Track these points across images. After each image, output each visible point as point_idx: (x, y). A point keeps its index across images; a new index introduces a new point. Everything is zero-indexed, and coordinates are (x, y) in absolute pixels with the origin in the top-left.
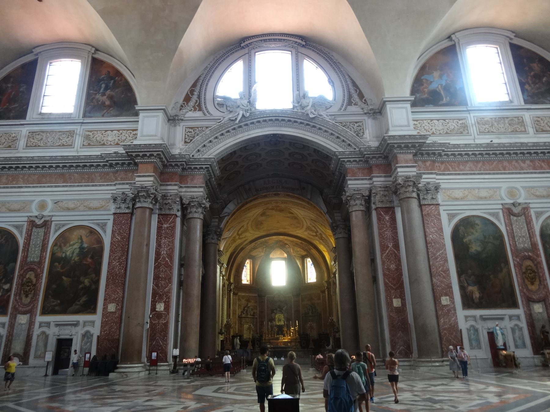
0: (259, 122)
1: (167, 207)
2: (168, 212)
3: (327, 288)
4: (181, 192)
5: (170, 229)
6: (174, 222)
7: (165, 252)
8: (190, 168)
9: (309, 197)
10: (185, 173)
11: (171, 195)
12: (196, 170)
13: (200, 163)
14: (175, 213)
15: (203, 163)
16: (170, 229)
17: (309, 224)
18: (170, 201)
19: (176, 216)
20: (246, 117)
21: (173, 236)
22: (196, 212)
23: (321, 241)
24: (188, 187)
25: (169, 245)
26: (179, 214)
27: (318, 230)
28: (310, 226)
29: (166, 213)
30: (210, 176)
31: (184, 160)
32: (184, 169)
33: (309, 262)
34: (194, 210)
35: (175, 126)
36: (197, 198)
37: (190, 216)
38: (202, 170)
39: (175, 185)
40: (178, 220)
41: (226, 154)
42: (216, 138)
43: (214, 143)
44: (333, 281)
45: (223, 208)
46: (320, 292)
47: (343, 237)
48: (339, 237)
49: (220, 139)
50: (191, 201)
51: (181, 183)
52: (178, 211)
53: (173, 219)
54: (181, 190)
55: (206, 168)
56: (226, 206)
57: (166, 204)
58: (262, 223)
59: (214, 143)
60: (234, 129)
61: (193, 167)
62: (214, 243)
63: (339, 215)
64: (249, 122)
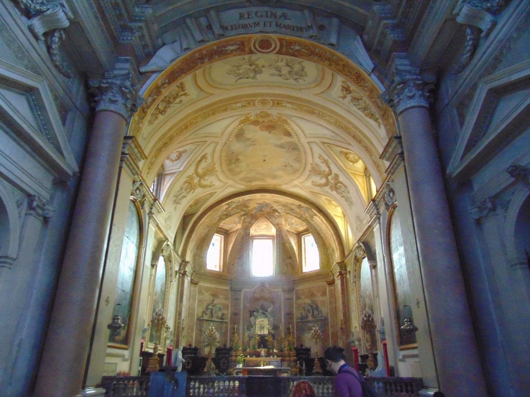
3: (341, 274)
9: (333, 40)
17: (316, 156)
23: (334, 193)
27: (333, 166)
28: (318, 161)
33: (309, 240)
44: (356, 257)
46: (325, 284)
47: (420, 107)
48: (409, 106)
62: (112, 111)
63: (407, 62)
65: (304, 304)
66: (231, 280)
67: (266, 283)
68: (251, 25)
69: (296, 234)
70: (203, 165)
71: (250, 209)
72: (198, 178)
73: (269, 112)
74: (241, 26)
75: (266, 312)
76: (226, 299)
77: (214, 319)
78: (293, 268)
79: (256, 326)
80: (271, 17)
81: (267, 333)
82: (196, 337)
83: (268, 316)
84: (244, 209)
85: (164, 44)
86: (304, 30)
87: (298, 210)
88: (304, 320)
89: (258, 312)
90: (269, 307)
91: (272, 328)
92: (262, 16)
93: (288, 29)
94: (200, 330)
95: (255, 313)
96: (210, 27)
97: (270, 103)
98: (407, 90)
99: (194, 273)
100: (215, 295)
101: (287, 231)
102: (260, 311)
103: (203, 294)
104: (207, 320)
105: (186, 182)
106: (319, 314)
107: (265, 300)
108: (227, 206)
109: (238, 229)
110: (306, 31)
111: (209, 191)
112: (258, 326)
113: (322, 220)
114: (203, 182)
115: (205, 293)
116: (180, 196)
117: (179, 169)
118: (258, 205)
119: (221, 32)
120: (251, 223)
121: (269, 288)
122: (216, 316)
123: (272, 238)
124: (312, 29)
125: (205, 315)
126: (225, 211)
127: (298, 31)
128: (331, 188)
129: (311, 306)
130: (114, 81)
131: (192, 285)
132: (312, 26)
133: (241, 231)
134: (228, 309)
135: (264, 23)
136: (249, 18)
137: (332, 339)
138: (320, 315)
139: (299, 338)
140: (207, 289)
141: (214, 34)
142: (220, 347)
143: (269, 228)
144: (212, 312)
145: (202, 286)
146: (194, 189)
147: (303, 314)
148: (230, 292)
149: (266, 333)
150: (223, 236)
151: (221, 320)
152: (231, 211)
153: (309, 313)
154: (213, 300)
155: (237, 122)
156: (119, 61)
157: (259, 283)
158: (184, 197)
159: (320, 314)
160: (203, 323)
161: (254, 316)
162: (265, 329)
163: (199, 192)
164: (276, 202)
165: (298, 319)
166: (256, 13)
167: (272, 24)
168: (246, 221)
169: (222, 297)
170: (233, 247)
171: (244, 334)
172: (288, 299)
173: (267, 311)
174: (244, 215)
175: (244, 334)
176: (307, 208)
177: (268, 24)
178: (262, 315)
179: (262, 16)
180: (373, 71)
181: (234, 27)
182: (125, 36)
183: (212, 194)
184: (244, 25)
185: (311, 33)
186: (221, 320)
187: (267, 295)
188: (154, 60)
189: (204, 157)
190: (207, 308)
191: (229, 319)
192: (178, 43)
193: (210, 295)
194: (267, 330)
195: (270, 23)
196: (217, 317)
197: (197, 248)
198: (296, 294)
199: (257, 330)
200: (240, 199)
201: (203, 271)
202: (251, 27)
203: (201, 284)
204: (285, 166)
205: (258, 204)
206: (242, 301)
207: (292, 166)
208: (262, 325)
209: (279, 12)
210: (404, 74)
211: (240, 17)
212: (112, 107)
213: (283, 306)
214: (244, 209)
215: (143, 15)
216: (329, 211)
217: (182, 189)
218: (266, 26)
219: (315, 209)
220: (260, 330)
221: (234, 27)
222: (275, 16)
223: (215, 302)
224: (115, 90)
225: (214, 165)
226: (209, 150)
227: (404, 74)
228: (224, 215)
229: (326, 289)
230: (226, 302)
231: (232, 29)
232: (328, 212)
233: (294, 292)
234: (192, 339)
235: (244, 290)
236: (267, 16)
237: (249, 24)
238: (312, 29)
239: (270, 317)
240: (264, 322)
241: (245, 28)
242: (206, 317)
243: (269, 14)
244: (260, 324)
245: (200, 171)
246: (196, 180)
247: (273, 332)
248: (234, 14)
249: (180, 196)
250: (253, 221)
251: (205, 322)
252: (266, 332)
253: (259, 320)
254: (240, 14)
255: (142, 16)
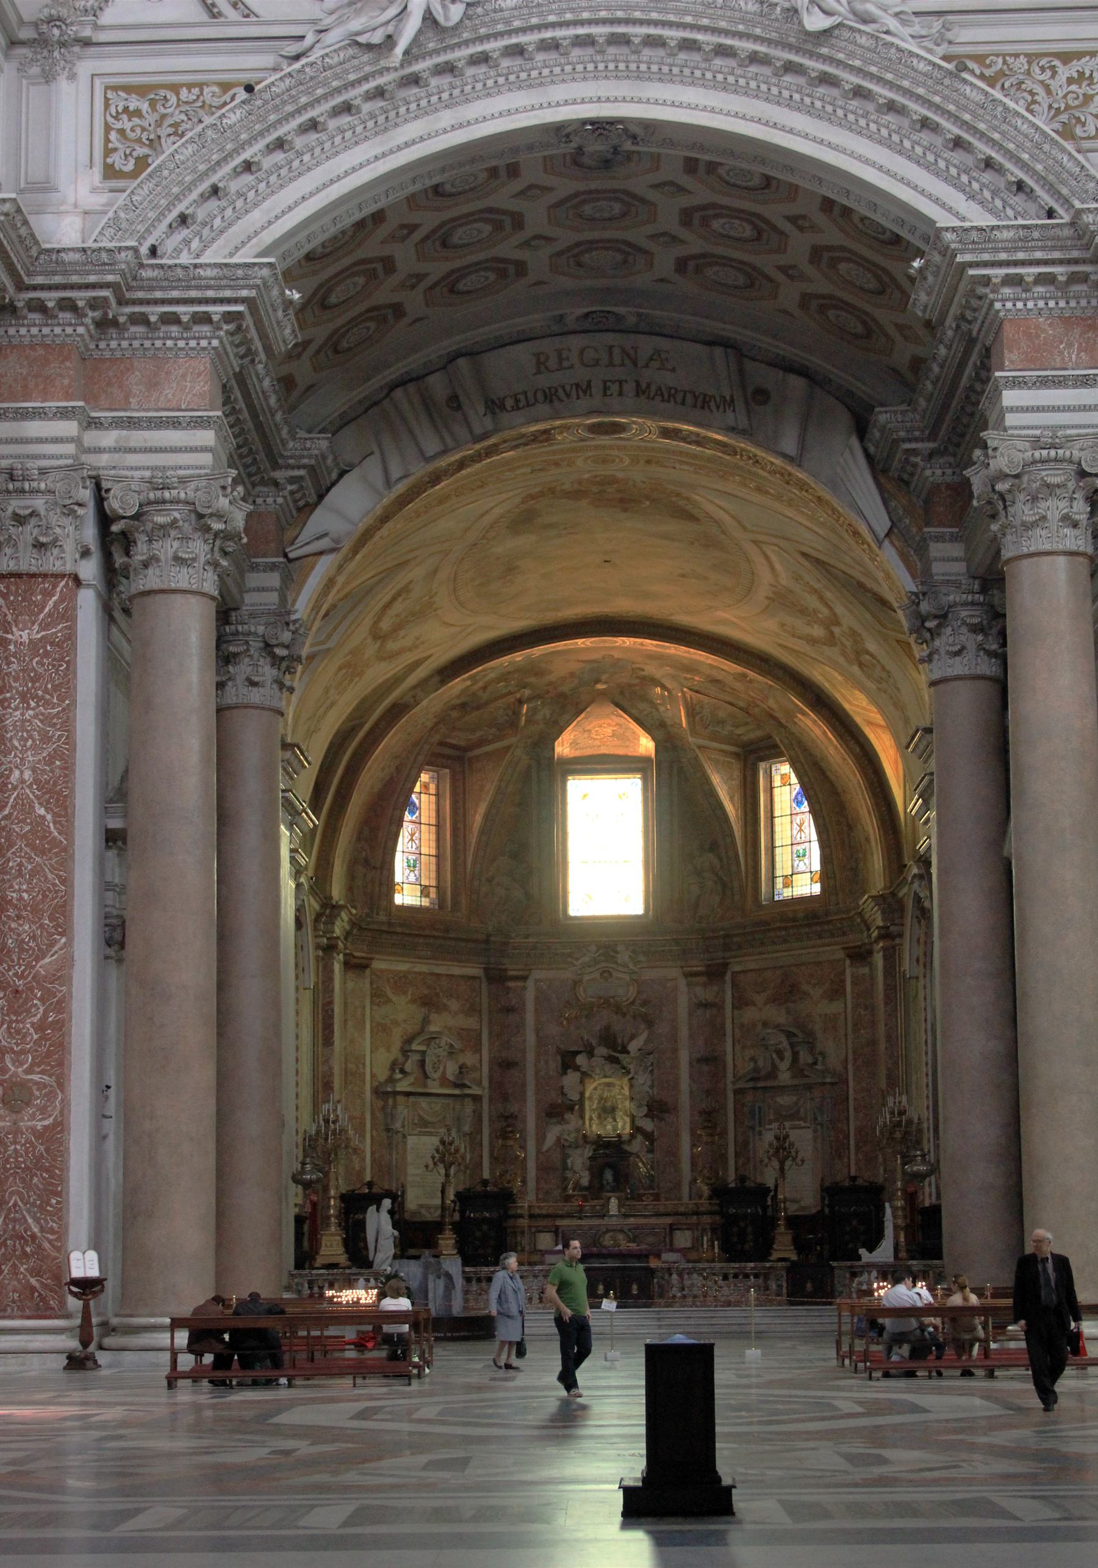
0: (518, 51)
1: (29, 532)
2: (28, 562)
4: (99, 450)
5: (47, 654)
6: (68, 615)
7: (27, 775)
8: (142, 320)
9: (789, 446)
10: (113, 343)
11: (43, 472)
12: (174, 330)
13: (193, 294)
14: (69, 568)
15: (210, 294)
16: (47, 654)
18: (39, 503)
19: (77, 581)
20: (444, 30)
21: (66, 688)
22: (178, 560)
24: (132, 424)
25: (46, 738)
26: (90, 570)
27: (840, 610)
29: (24, 568)
30: (249, 354)
31: (110, 278)
32: (105, 324)
34: (167, 548)
35: (48, 77)
36: (183, 481)
37: (151, 580)
38: (206, 329)
39: (64, 414)
40: (87, 603)
41: (333, 230)
42: (280, 144)
43: (269, 173)
45: (307, 509)
49: (300, 154)
50: (149, 503)
51: (91, 398)
52: (85, 553)
53: (62, 600)
54: (92, 438)
55: (228, 317)
56: (321, 497)
57: (20, 520)
58: (510, 570)
59: (269, 173)
60: (380, 93)
61: (154, 313)
64: (462, 54)
65: (765, 1024)
66: (487, 941)
67: (620, 948)
68: (568, 388)
69: (737, 755)
70: (398, 607)
71: (552, 677)
72: (379, 643)
73: (620, 475)
74: (540, 396)
75: (621, 1056)
76: (473, 1010)
77: (434, 1088)
78: (724, 886)
79: (587, 1103)
80: (623, 365)
81: (628, 1130)
82: (373, 1153)
83: (632, 1067)
84: (532, 680)
85: (342, 474)
86: (712, 404)
87: (738, 685)
88: (761, 1084)
89: (591, 1053)
90: (633, 1037)
91: (645, 1110)
92: (597, 363)
93: (669, 401)
94: (388, 1130)
95: (580, 1060)
96: (455, 403)
97: (621, 460)
98: (948, 630)
99: (355, 931)
100: (429, 1003)
101: (699, 747)
102: (601, 1051)
103: (388, 1001)
104: (408, 1094)
105: (340, 668)
106: (815, 1063)
107: (619, 1010)
108: (469, 683)
109: (508, 748)
110: (718, 407)
111: (409, 658)
112: (591, 1107)
113: (824, 733)
114: (391, 646)
115: (394, 998)
116: (321, 711)
117: (323, 643)
118: (582, 665)
119: (488, 423)
120: (556, 723)
121: (631, 966)
122: (436, 1076)
123: (640, 765)
124: (734, 411)
125: (399, 1076)
126: (458, 697)
127: (695, 406)
128: (844, 653)
129: (789, 1035)
130: (253, 629)
131: (350, 974)
132: (732, 400)
133: (519, 752)
134: (478, 1049)
135: (605, 382)
136: (561, 368)
137: (858, 1148)
138: (819, 1067)
139: (743, 1148)
140: (401, 982)
141: (471, 432)
142: (468, 1190)
143: (628, 734)
144: (422, 1063)
145: (382, 971)
146: (361, 674)
147: (760, 1064)
148: (484, 985)
149: (623, 1128)
150: (447, 771)
151: (457, 1092)
152: (480, 693)
153: (782, 1059)
154: (426, 1021)
155: (518, 500)
156: (255, 568)
157: (593, 948)
158: (333, 704)
159: (819, 1063)
160: (395, 1106)
161: (577, 1068)
162: (619, 1114)
163: (378, 673)
164: (652, 657)
165: (740, 1078)
166: (582, 352)
167: (626, 387)
168: (539, 717)
169: (454, 1005)
170: (487, 817)
171: (541, 1138)
172: (705, 1005)
173: (625, 1051)
174: (529, 699)
175: (541, 1138)
176: (771, 686)
177: (615, 388)
178: (608, 1067)
179: (597, 363)
180: (887, 535)
181: (522, 397)
182: (258, 496)
183: (416, 664)
184: (550, 389)
185: (730, 418)
186: (457, 1092)
187: (626, 993)
188: (320, 520)
189: (405, 590)
190: (405, 1052)
191: (485, 1083)
192: (377, 455)
193: (413, 1001)
194: (628, 1120)
195: (621, 383)
196: (444, 1081)
197: (359, 839)
198: (735, 985)
199: (591, 1119)
200: (518, 657)
201: (382, 918)
202: (568, 395)
203: (378, 965)
204: (683, 576)
205: (583, 661)
206: (530, 1018)
207: (706, 578)
208: (606, 1100)
209: (647, 345)
210: (944, 589)
211: (539, 363)
212: (255, 696)
213: (684, 1033)
214: (532, 680)
215: (305, 453)
216: (847, 706)
217: (327, 691)
218: (609, 393)
219: (800, 696)
220: (599, 1117)
221: (522, 397)
222: (635, 363)
223: (433, 1028)
224: (256, 645)
225: (431, 597)
226: (416, 573)
227: (945, 591)
228: (454, 708)
229: (843, 972)
230: (471, 1023)
231: (517, 407)
232: (844, 710)
233: (728, 977)
234: (363, 1160)
235: (536, 974)
236: (611, 364)
237: (563, 387)
238: (734, 411)
239: (636, 1073)
240: (616, 1090)
241: (551, 401)
242: (403, 1086)
243: (616, 351)
244: (601, 1098)
245: (385, 625)
246: (372, 649)
247: (648, 1125)
248: (522, 353)
249: (321, 711)
250: (566, 717)
251: (400, 1099)
252: (622, 1126)
253: (595, 1084)
254: (538, 355)
255: (302, 457)
